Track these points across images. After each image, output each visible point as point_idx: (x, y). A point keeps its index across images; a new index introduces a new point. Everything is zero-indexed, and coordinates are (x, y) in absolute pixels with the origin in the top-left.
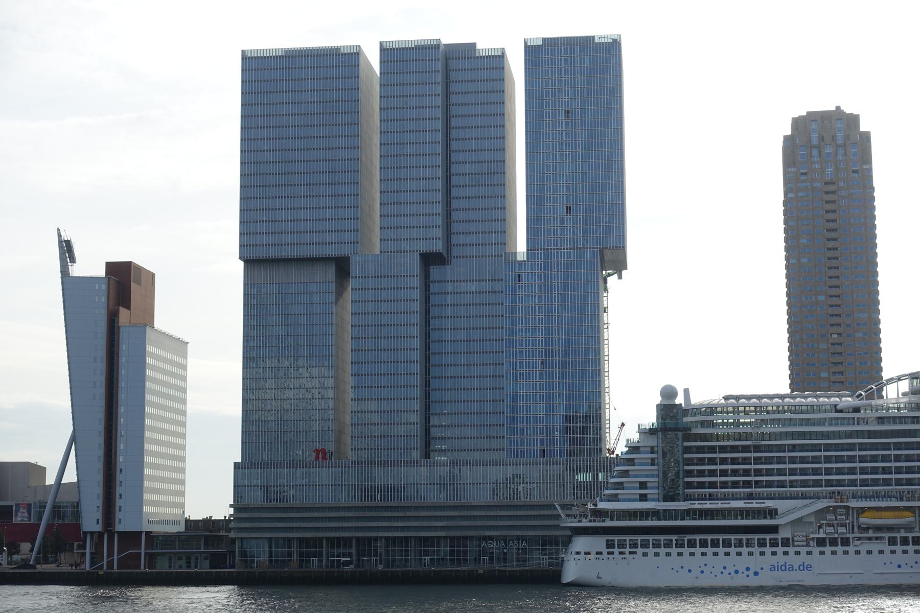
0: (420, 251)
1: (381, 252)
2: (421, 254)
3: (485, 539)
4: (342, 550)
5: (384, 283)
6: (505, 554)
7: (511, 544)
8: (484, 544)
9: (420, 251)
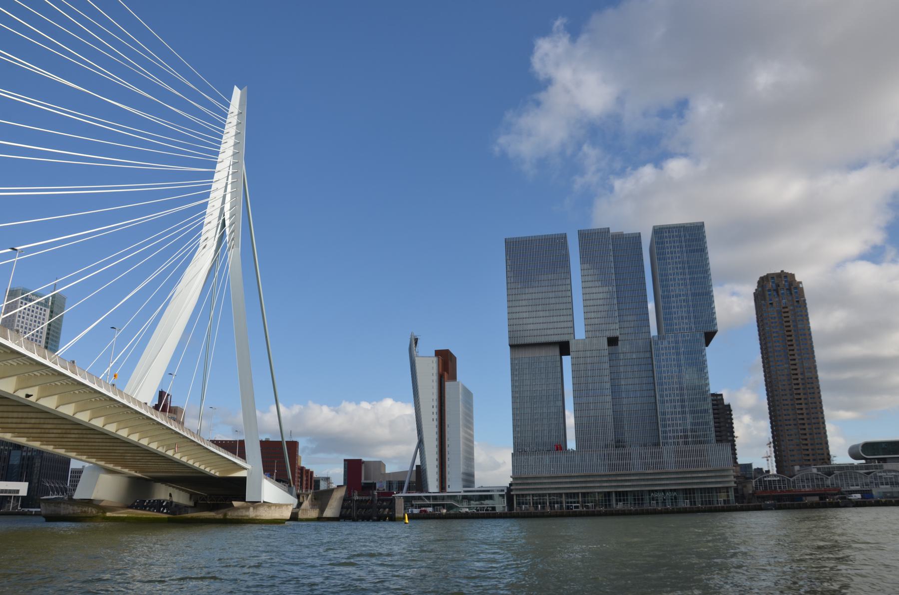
1: (586, 338)
2: (608, 338)
3: (653, 491)
5: (588, 354)
6: (664, 500)
7: (667, 494)
8: (652, 494)
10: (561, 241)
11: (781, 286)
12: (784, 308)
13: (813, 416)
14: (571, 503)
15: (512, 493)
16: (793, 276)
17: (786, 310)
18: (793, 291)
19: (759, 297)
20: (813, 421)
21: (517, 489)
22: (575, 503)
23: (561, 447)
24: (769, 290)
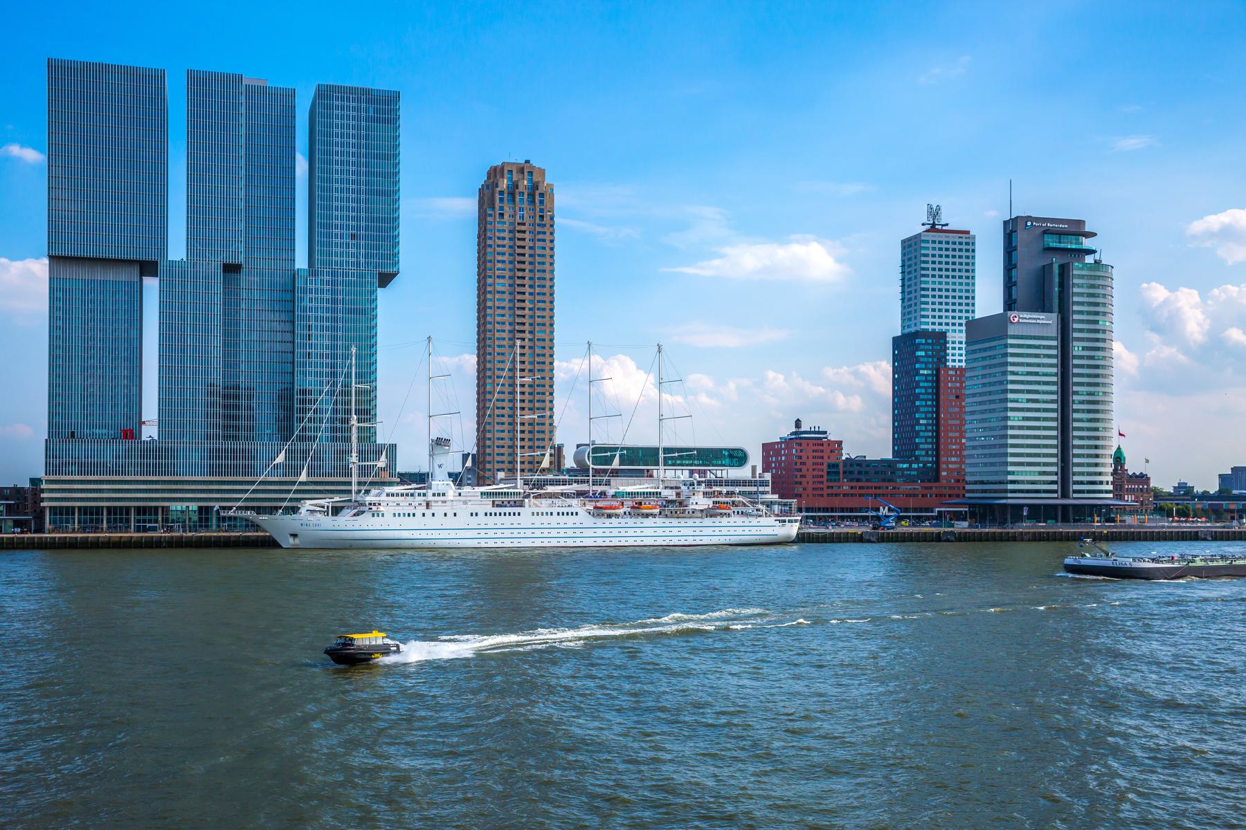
4: (147, 517)
11: (521, 188)
12: (519, 224)
13: (537, 397)
14: (144, 521)
15: (42, 504)
16: (542, 172)
17: (523, 228)
18: (537, 199)
19: (487, 197)
20: (537, 405)
21: (51, 499)
22: (150, 521)
23: (131, 434)
24: (501, 193)
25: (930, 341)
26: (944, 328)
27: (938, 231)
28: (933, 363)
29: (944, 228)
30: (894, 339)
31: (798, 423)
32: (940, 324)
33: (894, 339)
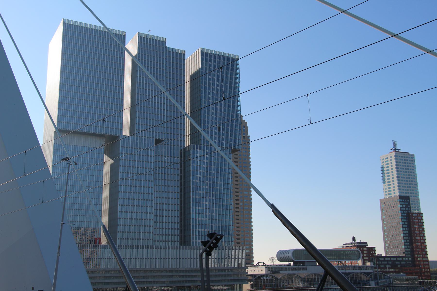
0: (155, 138)
2: (155, 140)
9: (155, 138)
10: (122, 38)
25: (404, 200)
26: (407, 195)
27: (397, 152)
28: (406, 210)
29: (400, 151)
30: (381, 201)
31: (354, 239)
32: (406, 193)
33: (381, 201)
